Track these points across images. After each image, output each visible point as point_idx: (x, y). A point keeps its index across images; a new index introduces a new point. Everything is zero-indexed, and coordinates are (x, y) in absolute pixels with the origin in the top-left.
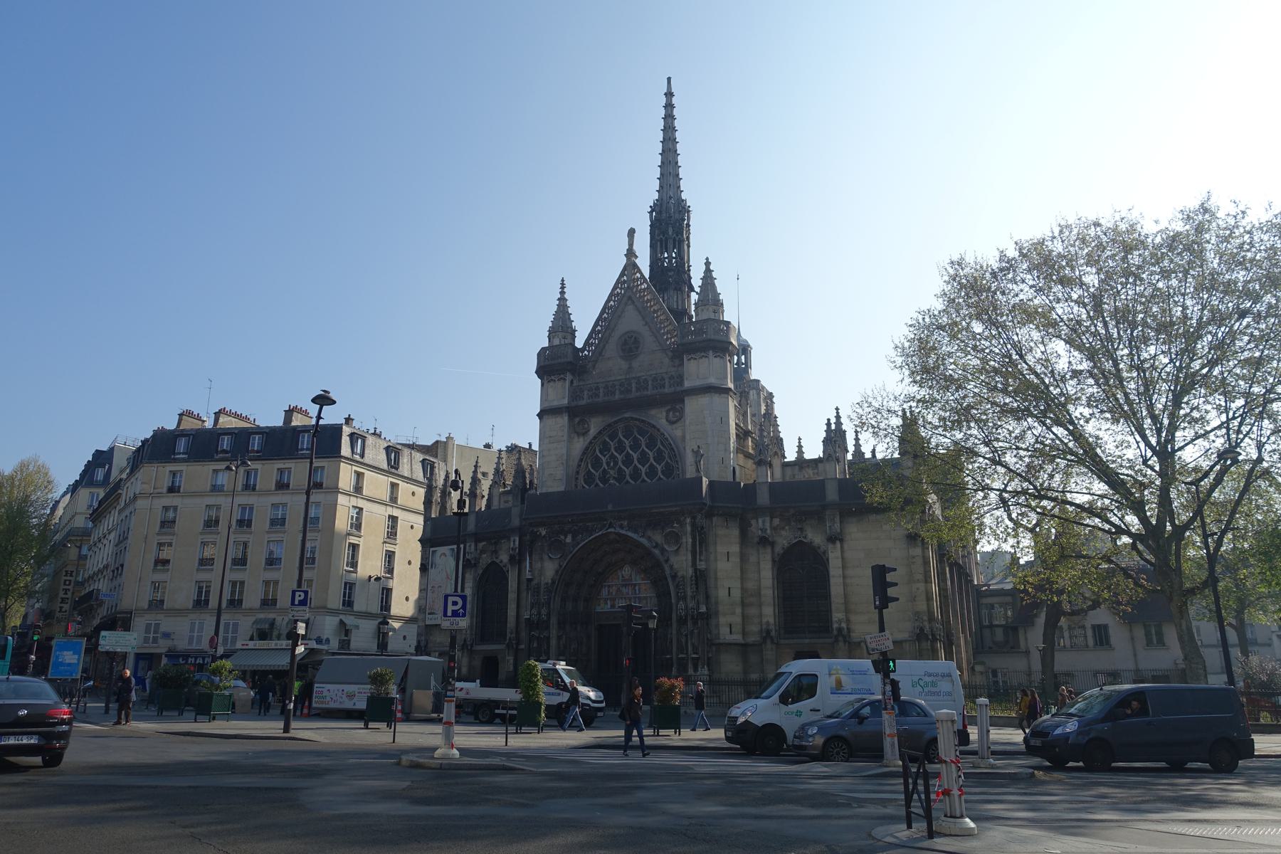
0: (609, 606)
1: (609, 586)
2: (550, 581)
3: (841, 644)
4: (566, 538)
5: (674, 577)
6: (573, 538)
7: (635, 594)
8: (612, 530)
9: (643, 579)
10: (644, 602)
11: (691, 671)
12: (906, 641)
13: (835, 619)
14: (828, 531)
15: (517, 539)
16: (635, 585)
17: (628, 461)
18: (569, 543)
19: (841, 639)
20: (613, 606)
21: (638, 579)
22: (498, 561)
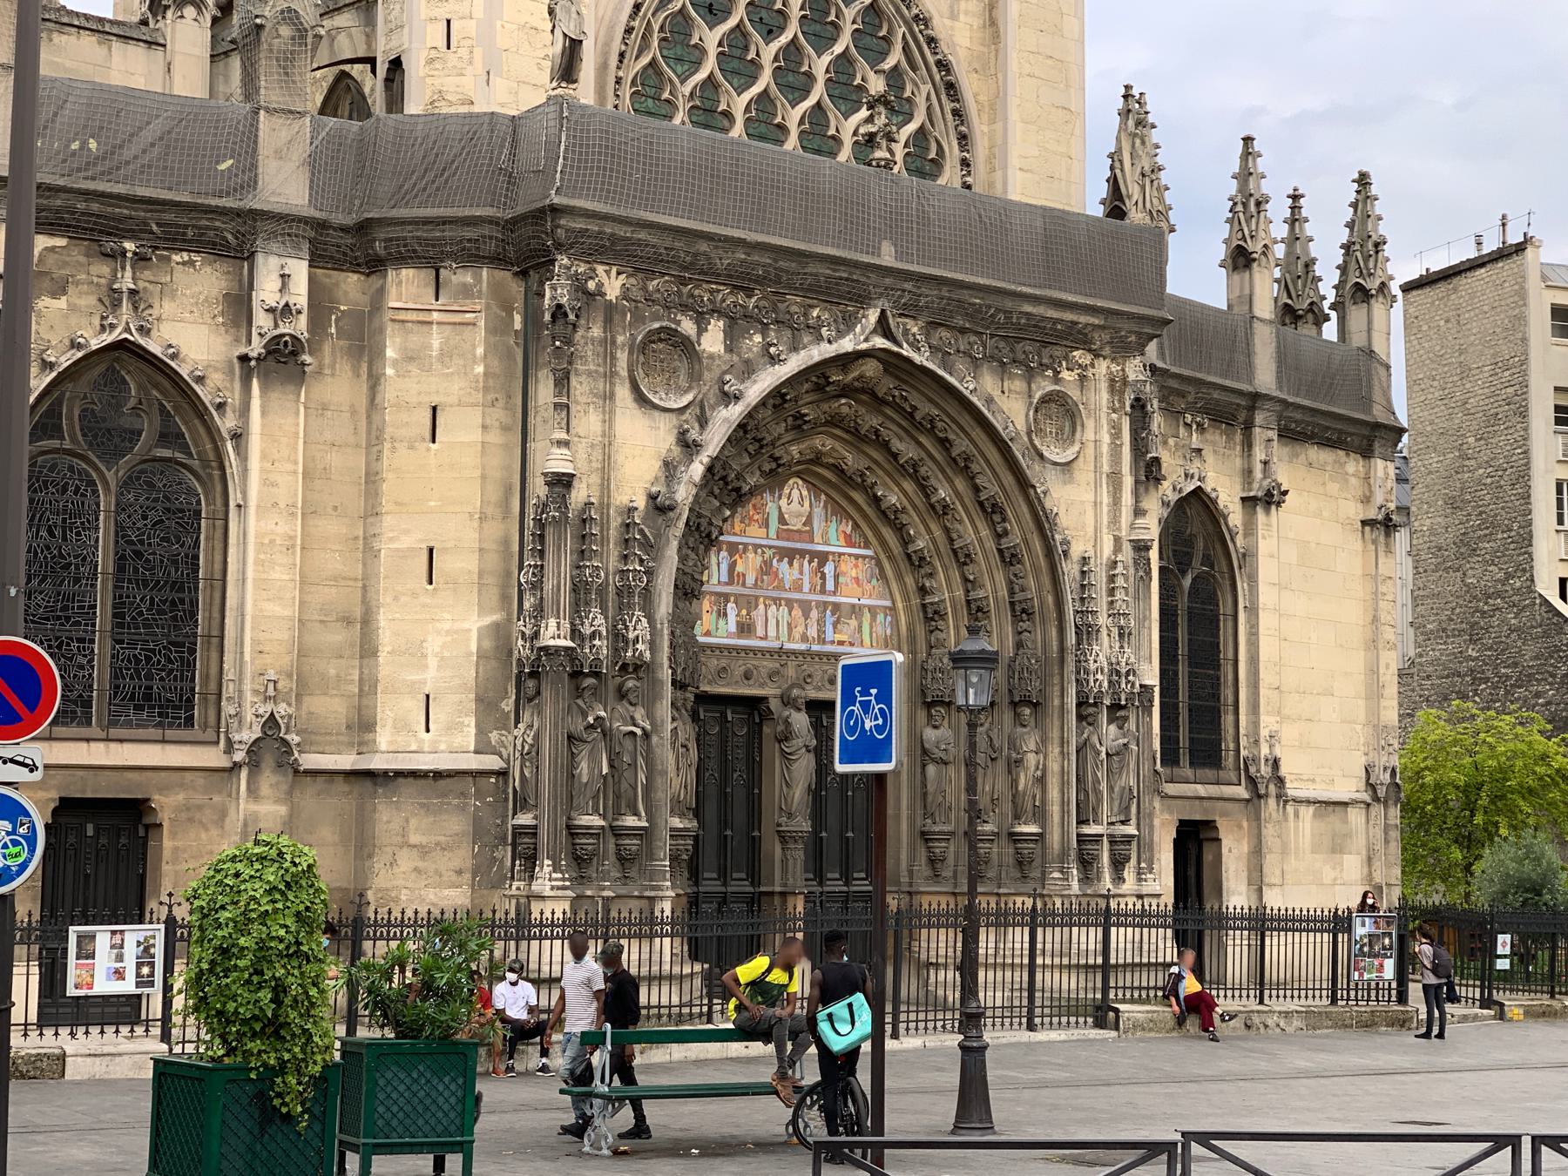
0: (733, 628)
1: (733, 549)
2: (641, 502)
3: (1272, 802)
4: (701, 331)
5: (1065, 553)
6: (732, 339)
7: (823, 591)
8: (880, 342)
9: (850, 544)
10: (854, 623)
11: (1107, 883)
12: (1354, 802)
13: (1264, 733)
14: (1258, 474)
15: (300, 270)
16: (823, 558)
17: (793, 78)
18: (711, 357)
19: (1272, 788)
20: (745, 628)
21: (831, 536)
22: (154, 347)
